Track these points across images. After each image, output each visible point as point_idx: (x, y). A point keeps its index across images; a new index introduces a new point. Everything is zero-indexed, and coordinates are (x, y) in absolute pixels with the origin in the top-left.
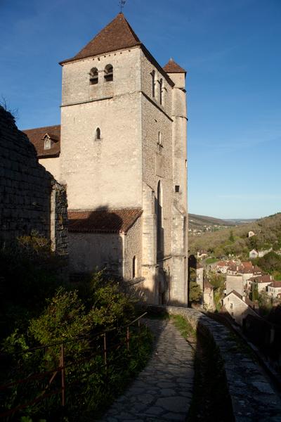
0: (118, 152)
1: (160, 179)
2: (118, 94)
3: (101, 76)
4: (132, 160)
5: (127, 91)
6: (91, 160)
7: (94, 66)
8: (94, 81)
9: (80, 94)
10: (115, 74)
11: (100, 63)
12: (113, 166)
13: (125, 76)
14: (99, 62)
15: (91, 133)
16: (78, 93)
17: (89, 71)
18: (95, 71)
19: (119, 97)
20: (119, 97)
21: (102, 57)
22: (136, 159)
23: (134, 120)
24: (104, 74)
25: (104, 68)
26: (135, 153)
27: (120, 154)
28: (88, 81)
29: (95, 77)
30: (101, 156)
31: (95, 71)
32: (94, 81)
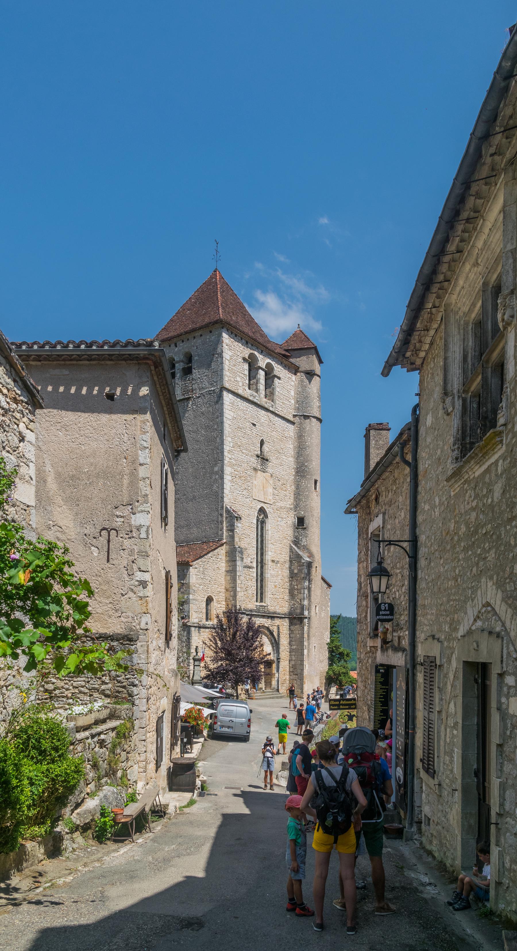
22: (217, 476)
26: (216, 469)
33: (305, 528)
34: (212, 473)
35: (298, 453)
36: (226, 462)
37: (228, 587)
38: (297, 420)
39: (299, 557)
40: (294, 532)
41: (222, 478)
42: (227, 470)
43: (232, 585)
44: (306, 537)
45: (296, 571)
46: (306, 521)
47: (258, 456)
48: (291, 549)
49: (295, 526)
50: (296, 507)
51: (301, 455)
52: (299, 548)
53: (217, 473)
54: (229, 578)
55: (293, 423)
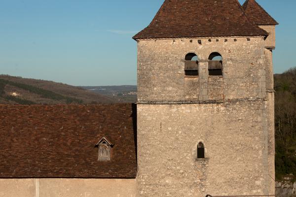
0: (233, 179)
2: (231, 97)
3: (203, 67)
5: (245, 96)
6: (191, 187)
8: (192, 72)
9: (170, 88)
13: (242, 74)
14: (201, 47)
15: (191, 150)
16: (168, 85)
21: (204, 40)
22: (259, 191)
26: (258, 183)
27: (237, 183)
28: (182, 71)
30: (208, 183)
32: (192, 72)
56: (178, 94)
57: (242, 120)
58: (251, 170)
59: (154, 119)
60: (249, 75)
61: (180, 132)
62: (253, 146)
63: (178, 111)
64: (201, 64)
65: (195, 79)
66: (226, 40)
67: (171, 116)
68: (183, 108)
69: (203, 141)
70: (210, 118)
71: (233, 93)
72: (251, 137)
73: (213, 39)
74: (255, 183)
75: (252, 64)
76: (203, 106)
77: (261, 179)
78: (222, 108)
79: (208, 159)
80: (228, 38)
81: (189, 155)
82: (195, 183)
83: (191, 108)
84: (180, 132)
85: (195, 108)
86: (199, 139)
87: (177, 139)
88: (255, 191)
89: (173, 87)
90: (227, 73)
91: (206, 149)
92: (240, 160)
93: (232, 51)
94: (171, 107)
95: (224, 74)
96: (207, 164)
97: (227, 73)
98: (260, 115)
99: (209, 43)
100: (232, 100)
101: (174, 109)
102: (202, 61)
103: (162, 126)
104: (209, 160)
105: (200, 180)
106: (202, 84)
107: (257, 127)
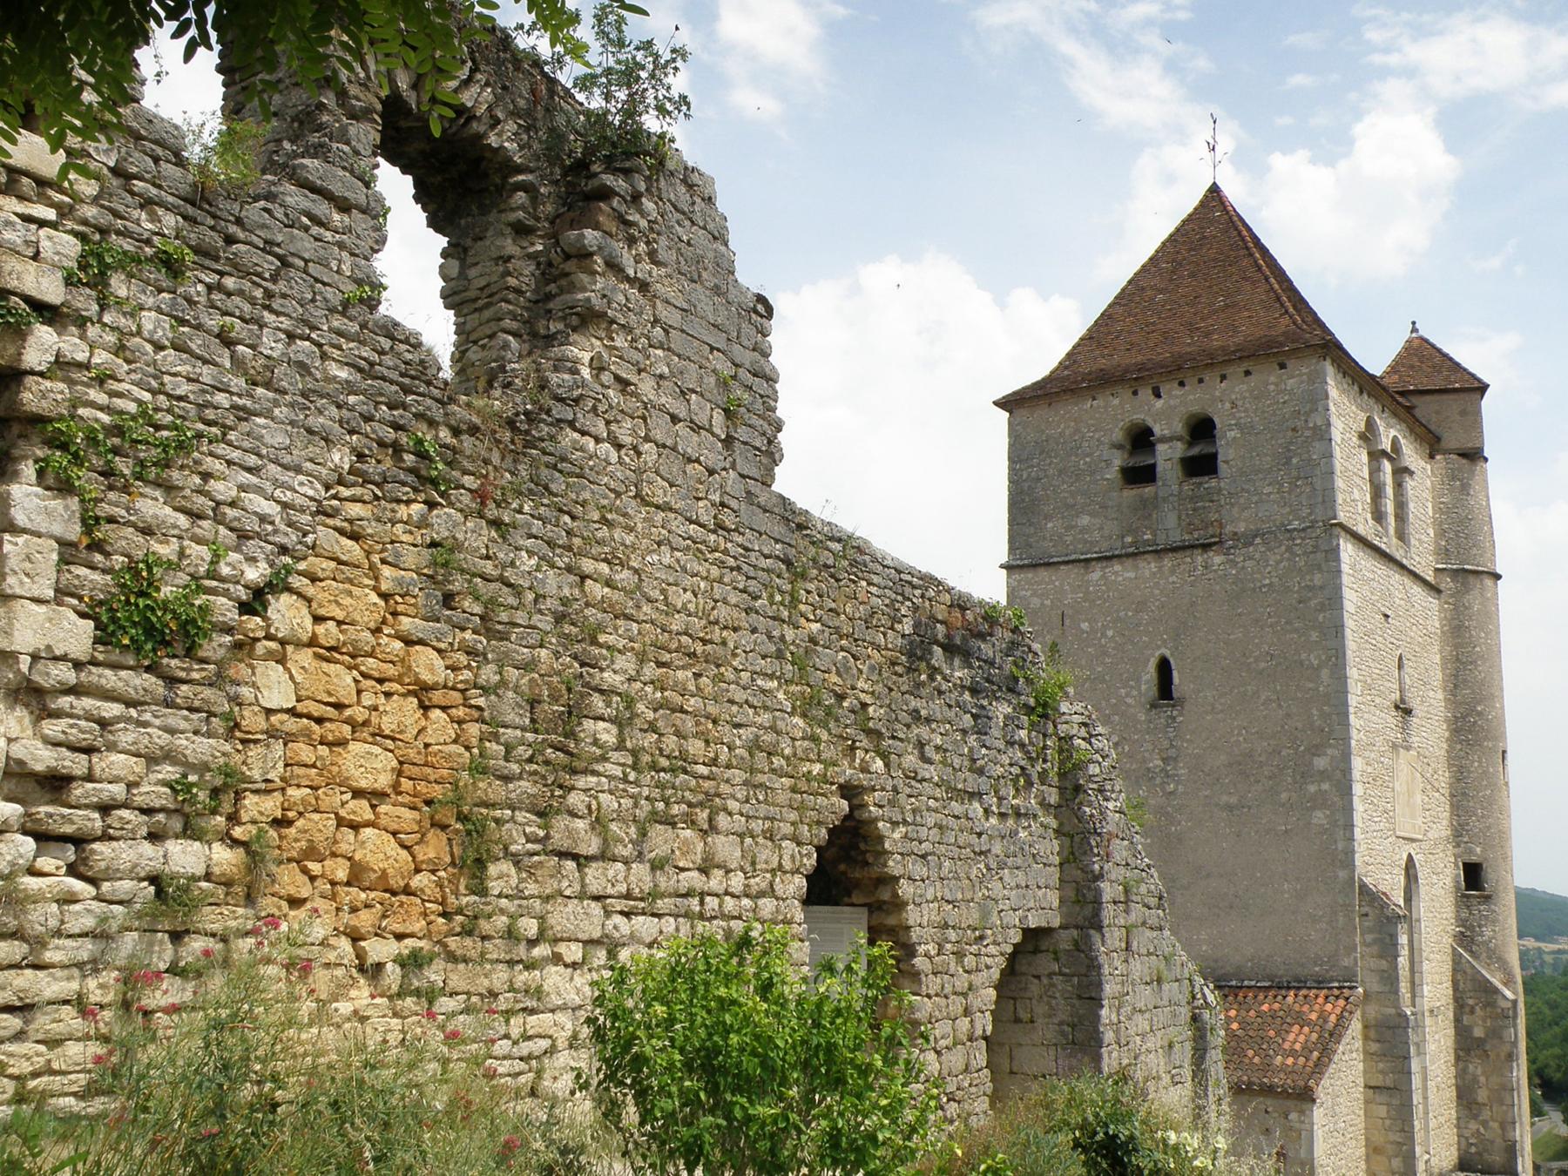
1: (1411, 848)
3: (1167, 456)
4: (1312, 788)
7: (1138, 417)
8: (1139, 475)
9: (1085, 520)
10: (1228, 447)
11: (1166, 413)
12: (1229, 808)
14: (1159, 403)
15: (1138, 680)
17: (1118, 435)
18: (1141, 439)
19: (1247, 540)
20: (1247, 540)
22: (1326, 786)
23: (1314, 636)
24: (1178, 450)
25: (1179, 427)
26: (1321, 763)
27: (1261, 765)
28: (1113, 473)
29: (1142, 460)
31: (1141, 439)
32: (1139, 475)
33: (1488, 898)
34: (1306, 775)
35: (1456, 676)
36: (1353, 743)
37: (1379, 1139)
38: (1447, 583)
39: (1490, 991)
40: (1457, 906)
41: (1347, 792)
42: (1357, 764)
43: (1397, 1137)
44: (1494, 922)
45: (1478, 1032)
46: (1490, 876)
47: (1397, 707)
48: (1457, 960)
49: (1458, 889)
50: (1459, 833)
51: (1465, 681)
52: (1471, 952)
53: (1324, 775)
54: (1382, 1111)
55: (1439, 591)
56: (1106, 533)
57: (1271, 585)
58: (1300, 725)
59: (1048, 602)
60: (1288, 462)
61: (1110, 633)
62: (1304, 656)
63: (1103, 577)
64: (1161, 448)
65: (1148, 490)
66: (1223, 378)
67: (1087, 593)
68: (1118, 567)
69: (1167, 653)
70: (1187, 588)
71: (1246, 514)
72: (1296, 630)
73: (1191, 383)
74: (1311, 763)
75: (1294, 430)
76: (1168, 562)
77: (1329, 751)
78: (1218, 559)
79: (1181, 702)
80: (1229, 371)
81: (1135, 693)
82: (1149, 769)
83: (1136, 568)
84: (1110, 633)
85: (1148, 567)
86: (1159, 647)
87: (1105, 654)
88: (1312, 788)
89: (1092, 514)
90: (1226, 462)
91: (1175, 674)
92: (1269, 700)
93: (1240, 403)
94: (1087, 568)
95: (1222, 467)
96: (1181, 714)
97: (1226, 462)
98: (1319, 568)
99: (1178, 392)
100: (1243, 534)
101: (1096, 575)
102: (1164, 440)
103: (1067, 622)
104: (1187, 706)
105: (1163, 759)
106: (1165, 500)
107: (1313, 603)
